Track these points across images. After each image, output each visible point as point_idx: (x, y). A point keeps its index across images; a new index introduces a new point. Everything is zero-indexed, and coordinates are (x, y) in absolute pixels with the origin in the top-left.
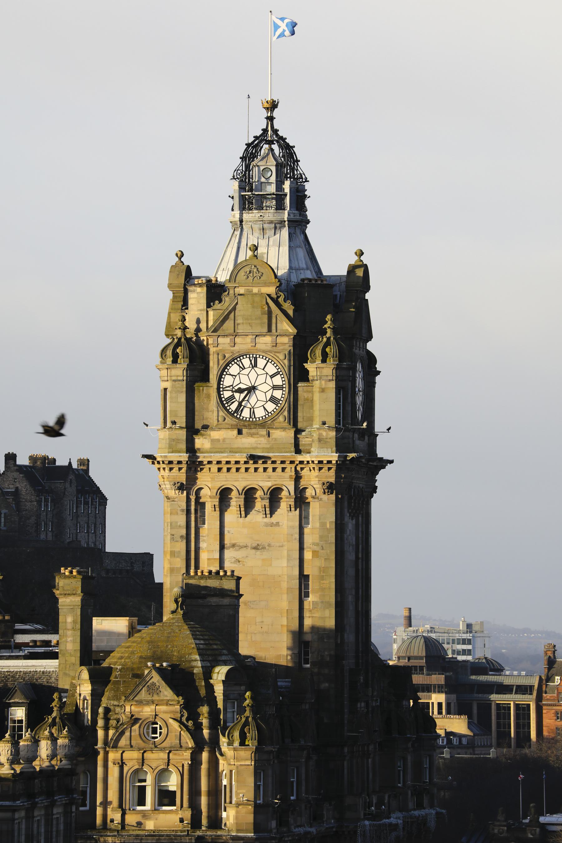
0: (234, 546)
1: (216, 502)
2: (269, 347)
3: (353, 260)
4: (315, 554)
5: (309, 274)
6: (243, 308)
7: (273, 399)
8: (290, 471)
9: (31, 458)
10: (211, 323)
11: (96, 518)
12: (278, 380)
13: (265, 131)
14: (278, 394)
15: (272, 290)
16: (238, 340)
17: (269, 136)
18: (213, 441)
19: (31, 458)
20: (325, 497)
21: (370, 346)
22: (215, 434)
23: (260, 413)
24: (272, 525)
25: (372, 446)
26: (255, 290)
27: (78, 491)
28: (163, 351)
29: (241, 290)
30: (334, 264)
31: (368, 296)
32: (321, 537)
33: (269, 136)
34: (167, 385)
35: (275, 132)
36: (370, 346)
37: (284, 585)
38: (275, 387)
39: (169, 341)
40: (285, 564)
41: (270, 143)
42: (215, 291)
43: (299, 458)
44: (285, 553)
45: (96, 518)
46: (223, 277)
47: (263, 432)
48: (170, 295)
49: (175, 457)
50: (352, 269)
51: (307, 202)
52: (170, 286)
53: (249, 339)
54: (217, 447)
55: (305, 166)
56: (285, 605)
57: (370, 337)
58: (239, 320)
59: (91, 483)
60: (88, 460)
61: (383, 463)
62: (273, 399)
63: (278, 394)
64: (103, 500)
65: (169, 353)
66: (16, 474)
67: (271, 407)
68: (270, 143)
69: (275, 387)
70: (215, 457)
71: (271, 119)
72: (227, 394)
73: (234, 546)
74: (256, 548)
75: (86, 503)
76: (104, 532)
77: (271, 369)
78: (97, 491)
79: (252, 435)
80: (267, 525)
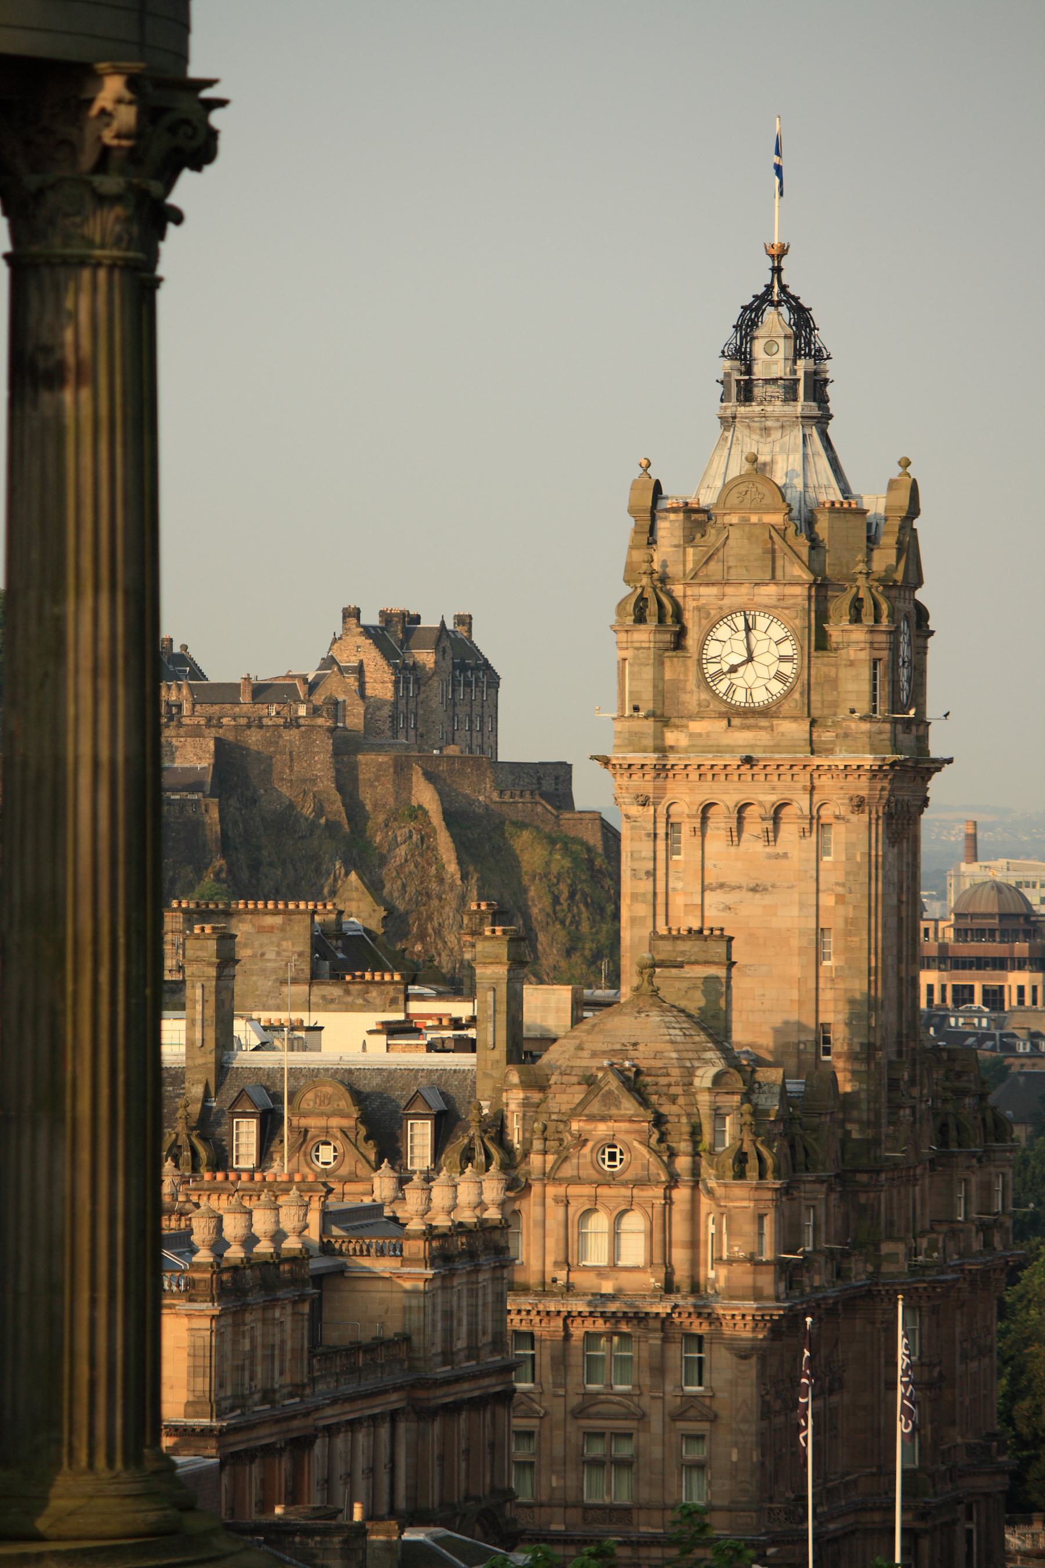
0: (722, 886)
1: (697, 823)
2: (773, 601)
4: (840, 899)
6: (737, 542)
7: (779, 676)
8: (803, 779)
9: (382, 613)
10: (690, 566)
11: (482, 707)
12: (787, 649)
13: (769, 288)
14: (787, 668)
15: (777, 519)
16: (729, 590)
17: (775, 295)
18: (691, 735)
19: (382, 613)
20: (854, 818)
21: (920, 595)
22: (695, 726)
23: (760, 697)
24: (777, 856)
25: (922, 740)
26: (754, 519)
27: (455, 666)
28: (621, 605)
29: (734, 519)
32: (848, 874)
33: (775, 295)
34: (628, 654)
35: (783, 288)
36: (920, 595)
37: (795, 942)
38: (782, 659)
39: (628, 590)
40: (795, 911)
42: (697, 519)
43: (817, 761)
44: (796, 897)
45: (482, 707)
46: (707, 498)
47: (764, 722)
48: (630, 522)
49: (636, 758)
51: (830, 389)
52: (632, 511)
53: (744, 590)
55: (824, 337)
56: (796, 971)
58: (732, 562)
59: (475, 652)
60: (470, 617)
61: (939, 764)
62: (779, 676)
63: (787, 668)
64: (494, 681)
65: (630, 608)
66: (362, 640)
67: (777, 687)
69: (782, 659)
71: (777, 270)
72: (712, 669)
73: (722, 886)
74: (754, 890)
75: (468, 684)
76: (495, 729)
77: (777, 631)
78: (487, 666)
79: (748, 728)
80: (770, 857)
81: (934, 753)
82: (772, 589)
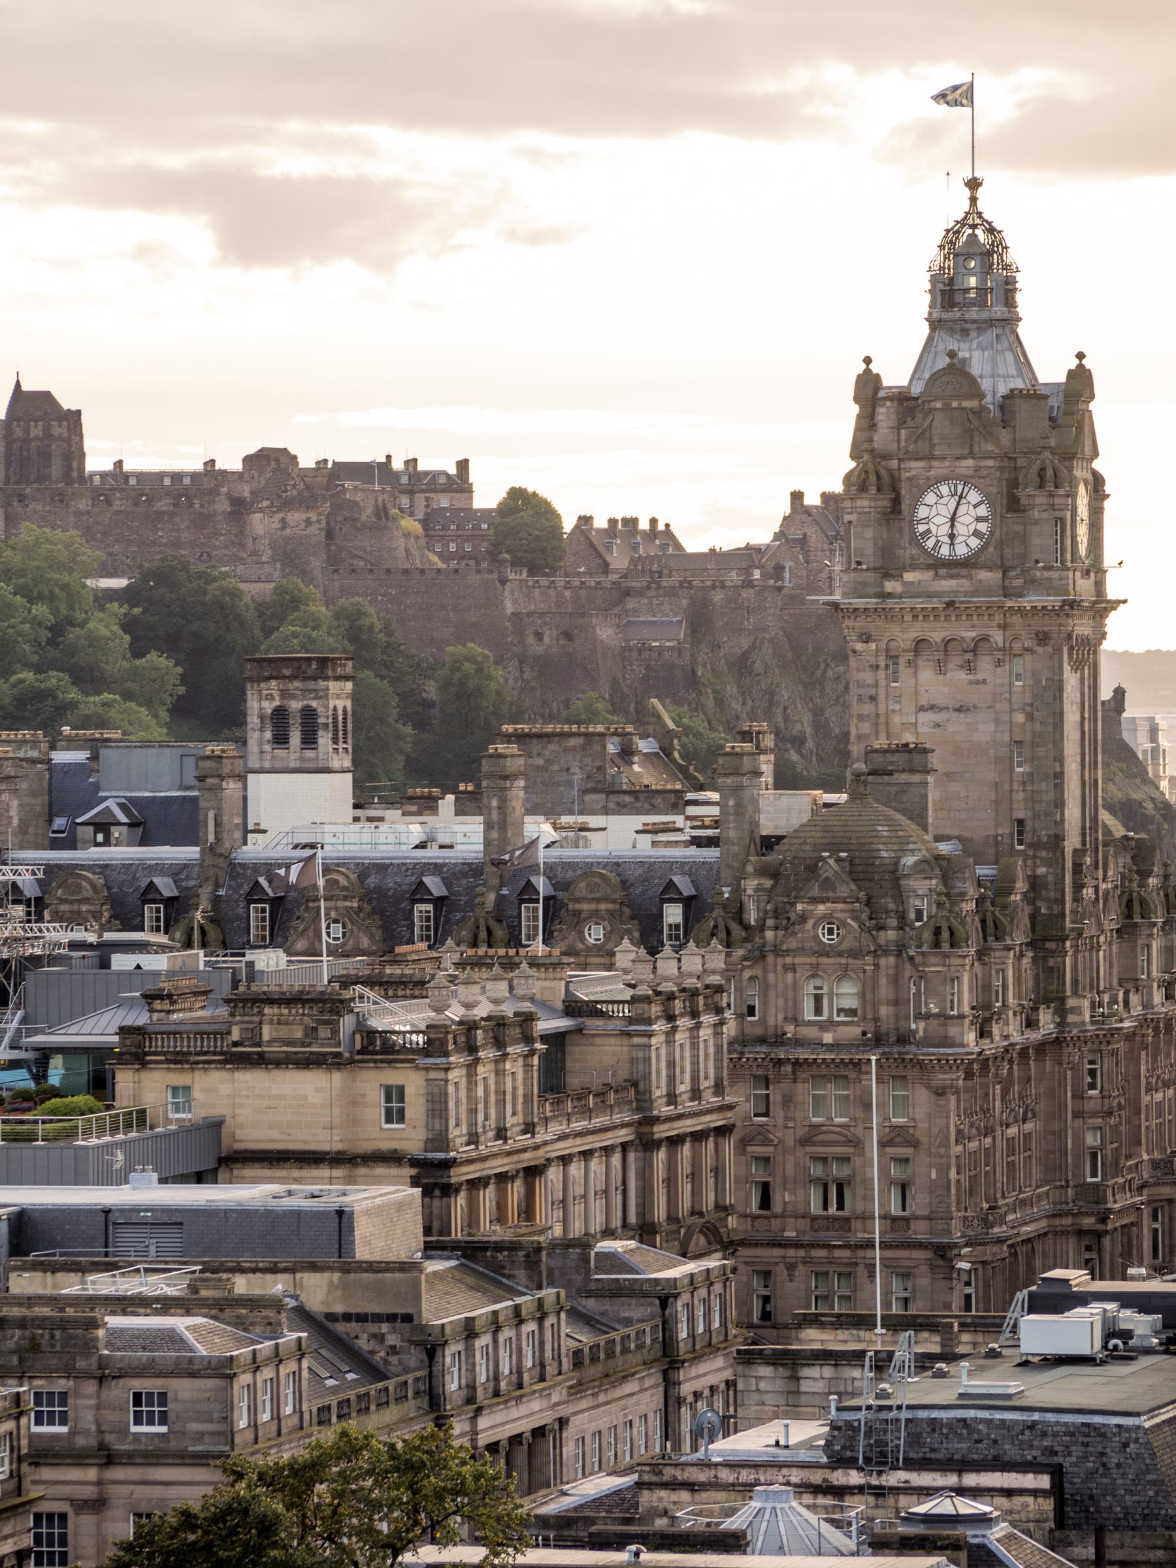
0: (932, 707)
2: (970, 472)
3: (1073, 363)
5: (1019, 384)
7: (976, 533)
12: (983, 511)
14: (983, 527)
16: (935, 464)
20: (1040, 650)
21: (1097, 465)
22: (909, 576)
23: (961, 550)
24: (977, 682)
25: (1100, 585)
26: (955, 404)
30: (1051, 370)
31: (1092, 406)
32: (1035, 696)
35: (980, 215)
36: (1097, 465)
38: (979, 519)
40: (990, 727)
41: (974, 227)
47: (964, 572)
50: (1071, 373)
51: (1019, 297)
52: (857, 399)
53: (947, 463)
54: (913, 591)
57: (1095, 454)
58: (936, 440)
61: (1115, 604)
62: (976, 533)
63: (983, 527)
67: (974, 543)
68: (974, 227)
69: (979, 519)
70: (908, 603)
71: (973, 200)
73: (932, 707)
74: (959, 710)
79: (952, 577)
80: (971, 682)
81: (1112, 593)
82: (970, 462)
